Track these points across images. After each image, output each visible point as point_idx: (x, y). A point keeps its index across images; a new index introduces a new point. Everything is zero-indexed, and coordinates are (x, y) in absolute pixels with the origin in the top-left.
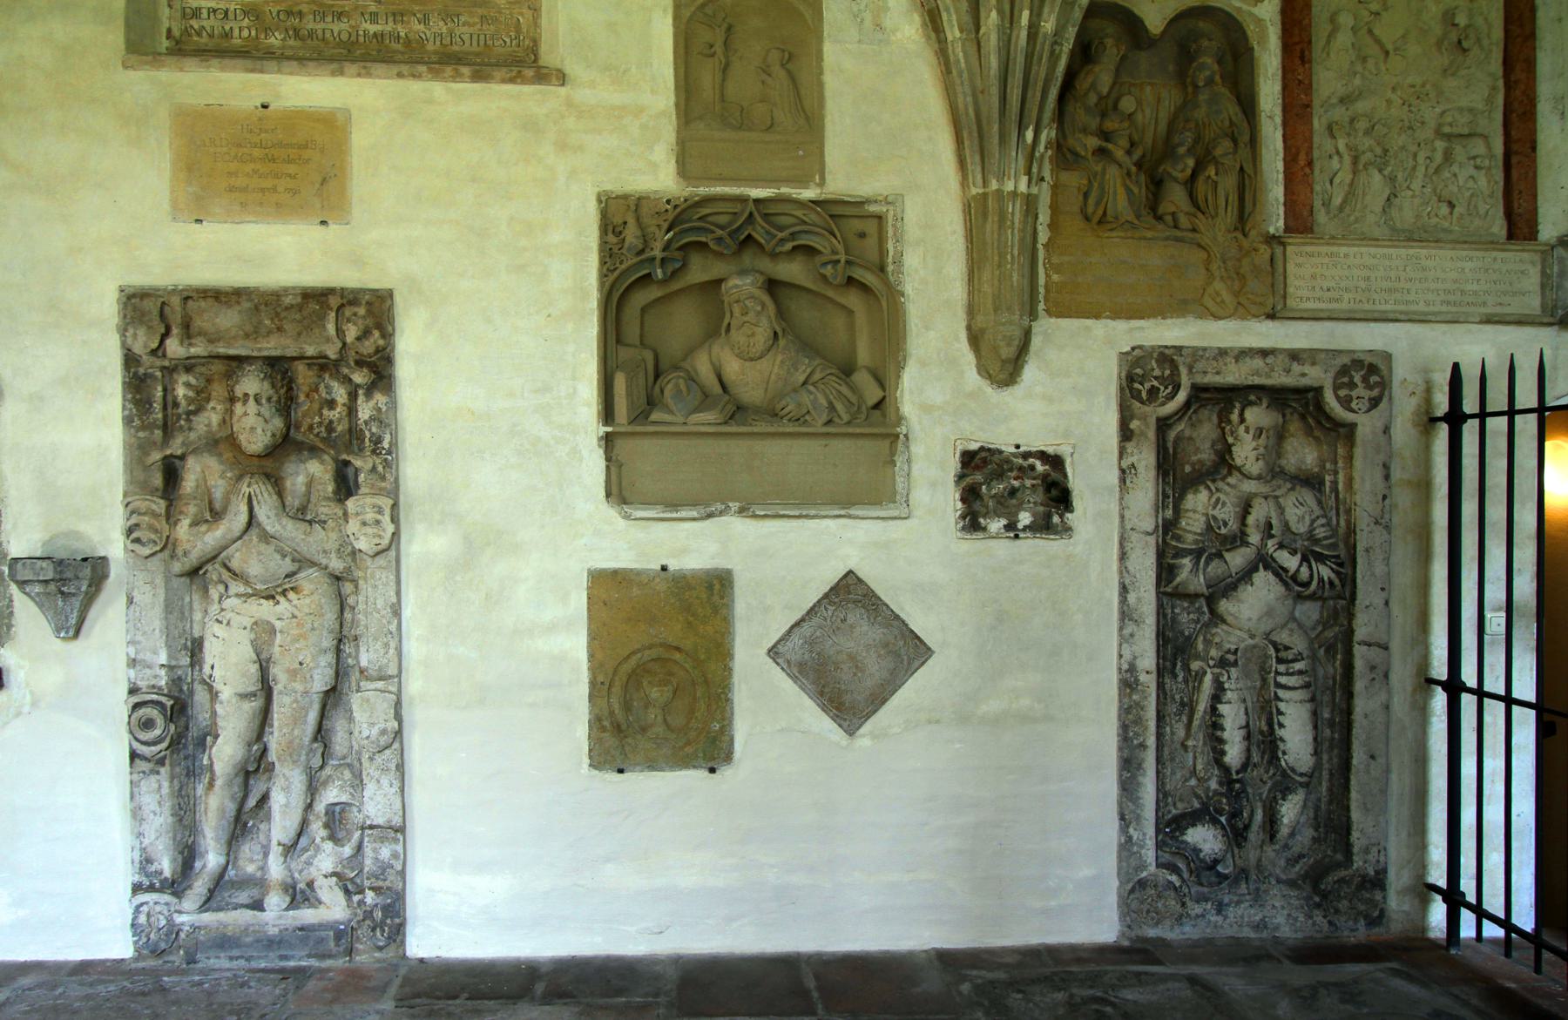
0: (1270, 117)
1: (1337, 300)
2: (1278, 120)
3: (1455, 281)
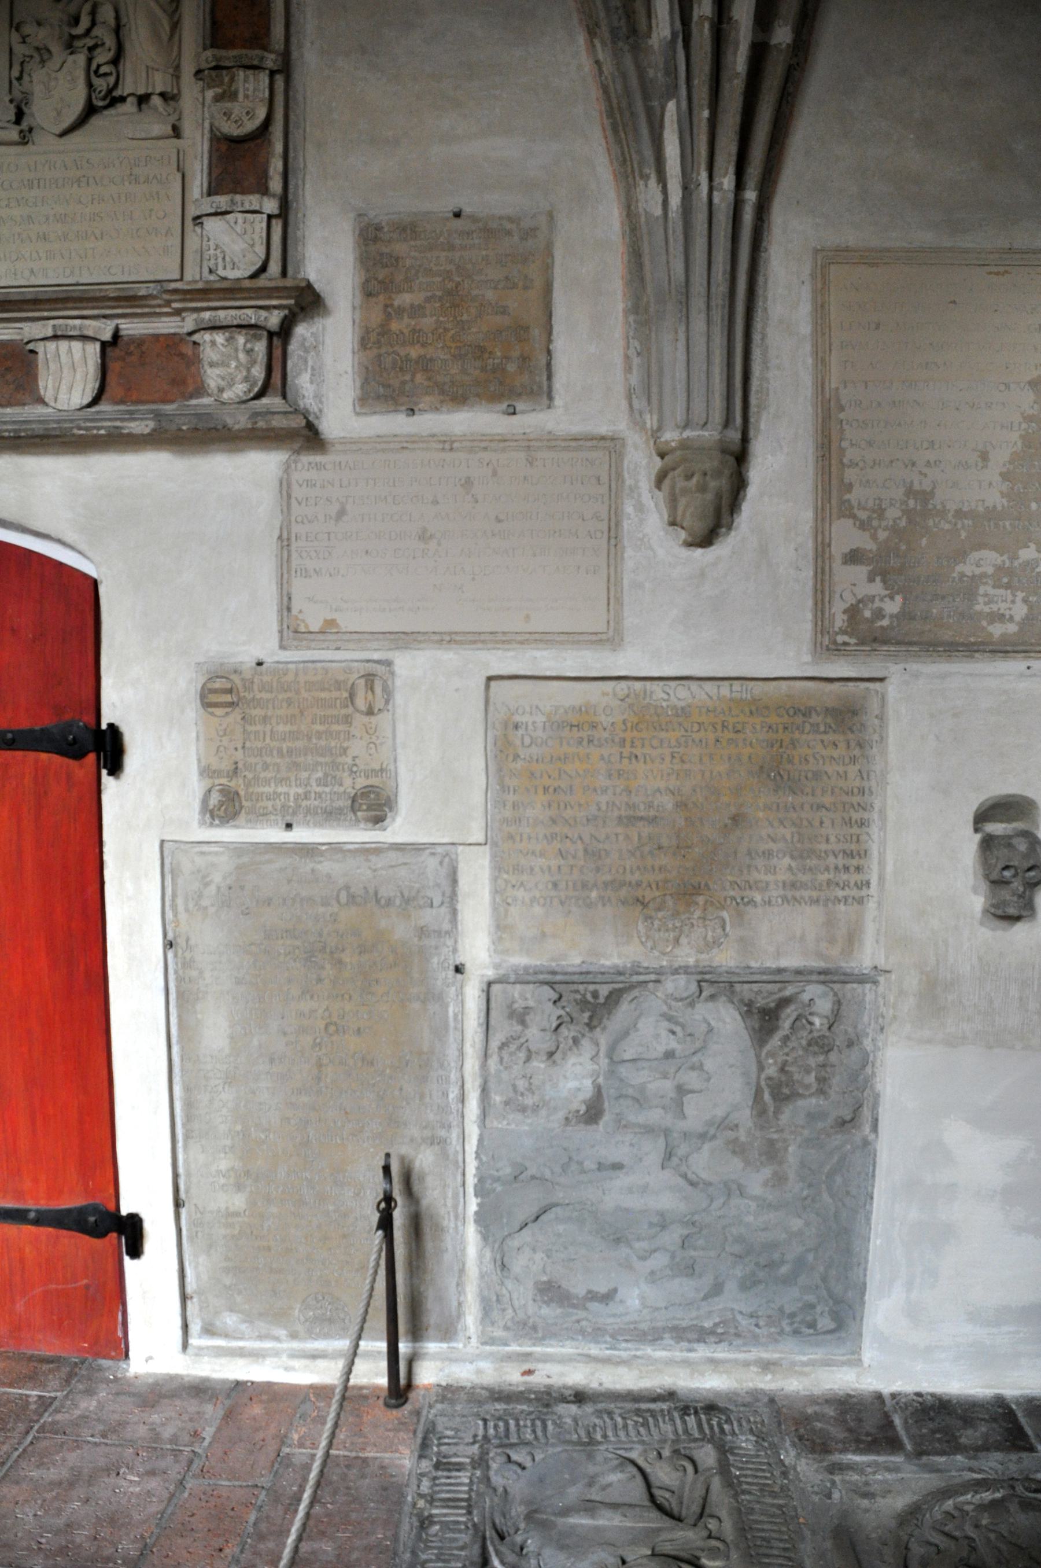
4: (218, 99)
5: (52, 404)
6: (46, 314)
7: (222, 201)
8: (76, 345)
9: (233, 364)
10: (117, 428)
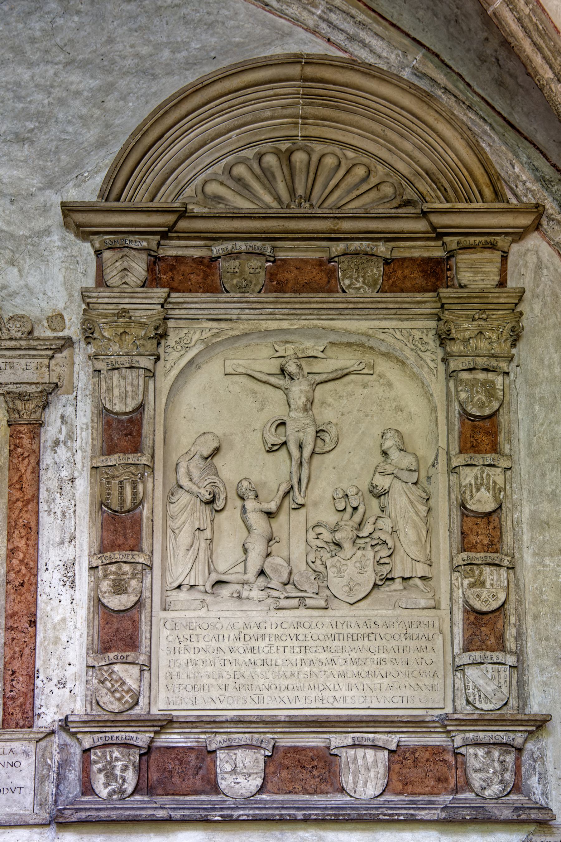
4: (472, 585)
5: (352, 794)
6: (350, 730)
7: (477, 655)
8: (370, 753)
9: (491, 771)
10: (412, 815)
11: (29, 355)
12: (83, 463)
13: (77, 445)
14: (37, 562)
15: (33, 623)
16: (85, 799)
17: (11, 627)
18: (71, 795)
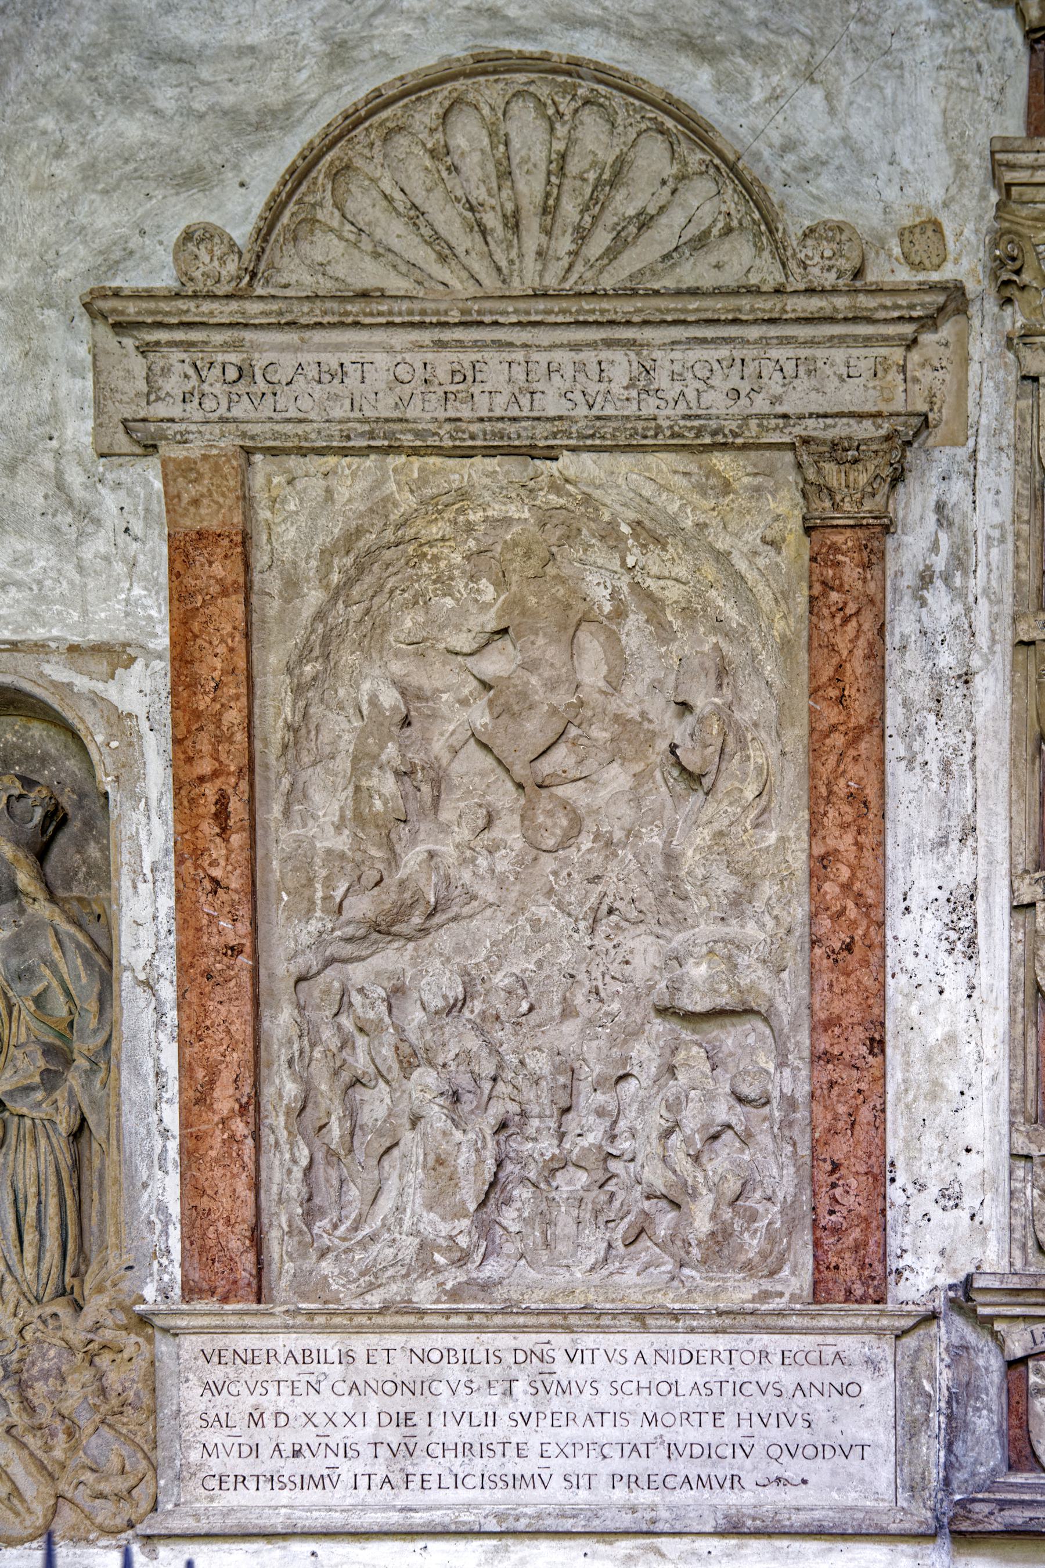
0: (148, 985)
1: (320, 1482)
2: (168, 992)
3: (652, 1420)
11: (855, 338)
12: (993, 633)
13: (977, 584)
14: (881, 890)
15: (877, 1045)
16: (1019, 1478)
17: (826, 1053)
18: (982, 1470)
